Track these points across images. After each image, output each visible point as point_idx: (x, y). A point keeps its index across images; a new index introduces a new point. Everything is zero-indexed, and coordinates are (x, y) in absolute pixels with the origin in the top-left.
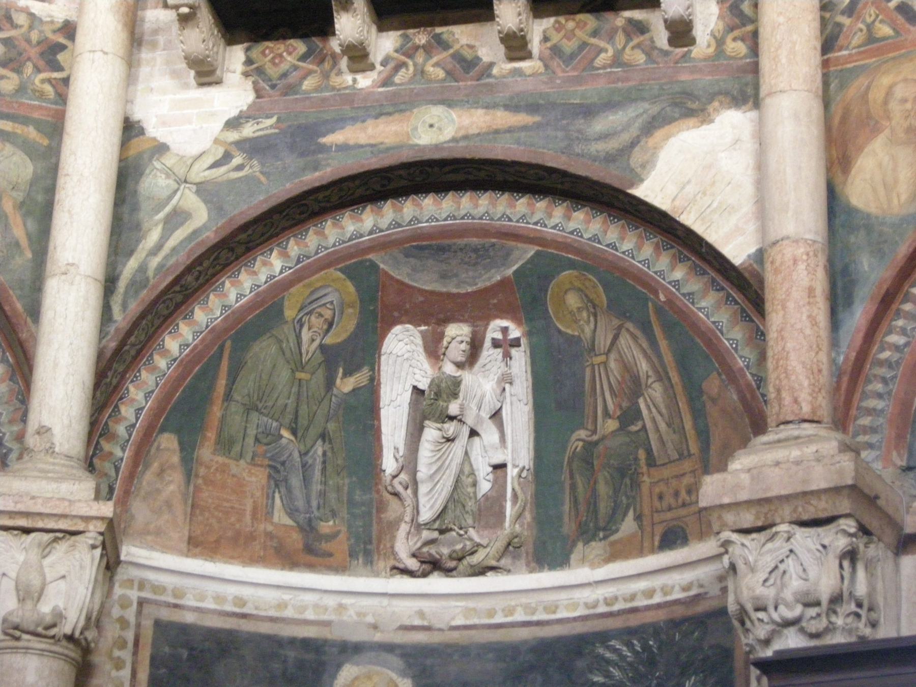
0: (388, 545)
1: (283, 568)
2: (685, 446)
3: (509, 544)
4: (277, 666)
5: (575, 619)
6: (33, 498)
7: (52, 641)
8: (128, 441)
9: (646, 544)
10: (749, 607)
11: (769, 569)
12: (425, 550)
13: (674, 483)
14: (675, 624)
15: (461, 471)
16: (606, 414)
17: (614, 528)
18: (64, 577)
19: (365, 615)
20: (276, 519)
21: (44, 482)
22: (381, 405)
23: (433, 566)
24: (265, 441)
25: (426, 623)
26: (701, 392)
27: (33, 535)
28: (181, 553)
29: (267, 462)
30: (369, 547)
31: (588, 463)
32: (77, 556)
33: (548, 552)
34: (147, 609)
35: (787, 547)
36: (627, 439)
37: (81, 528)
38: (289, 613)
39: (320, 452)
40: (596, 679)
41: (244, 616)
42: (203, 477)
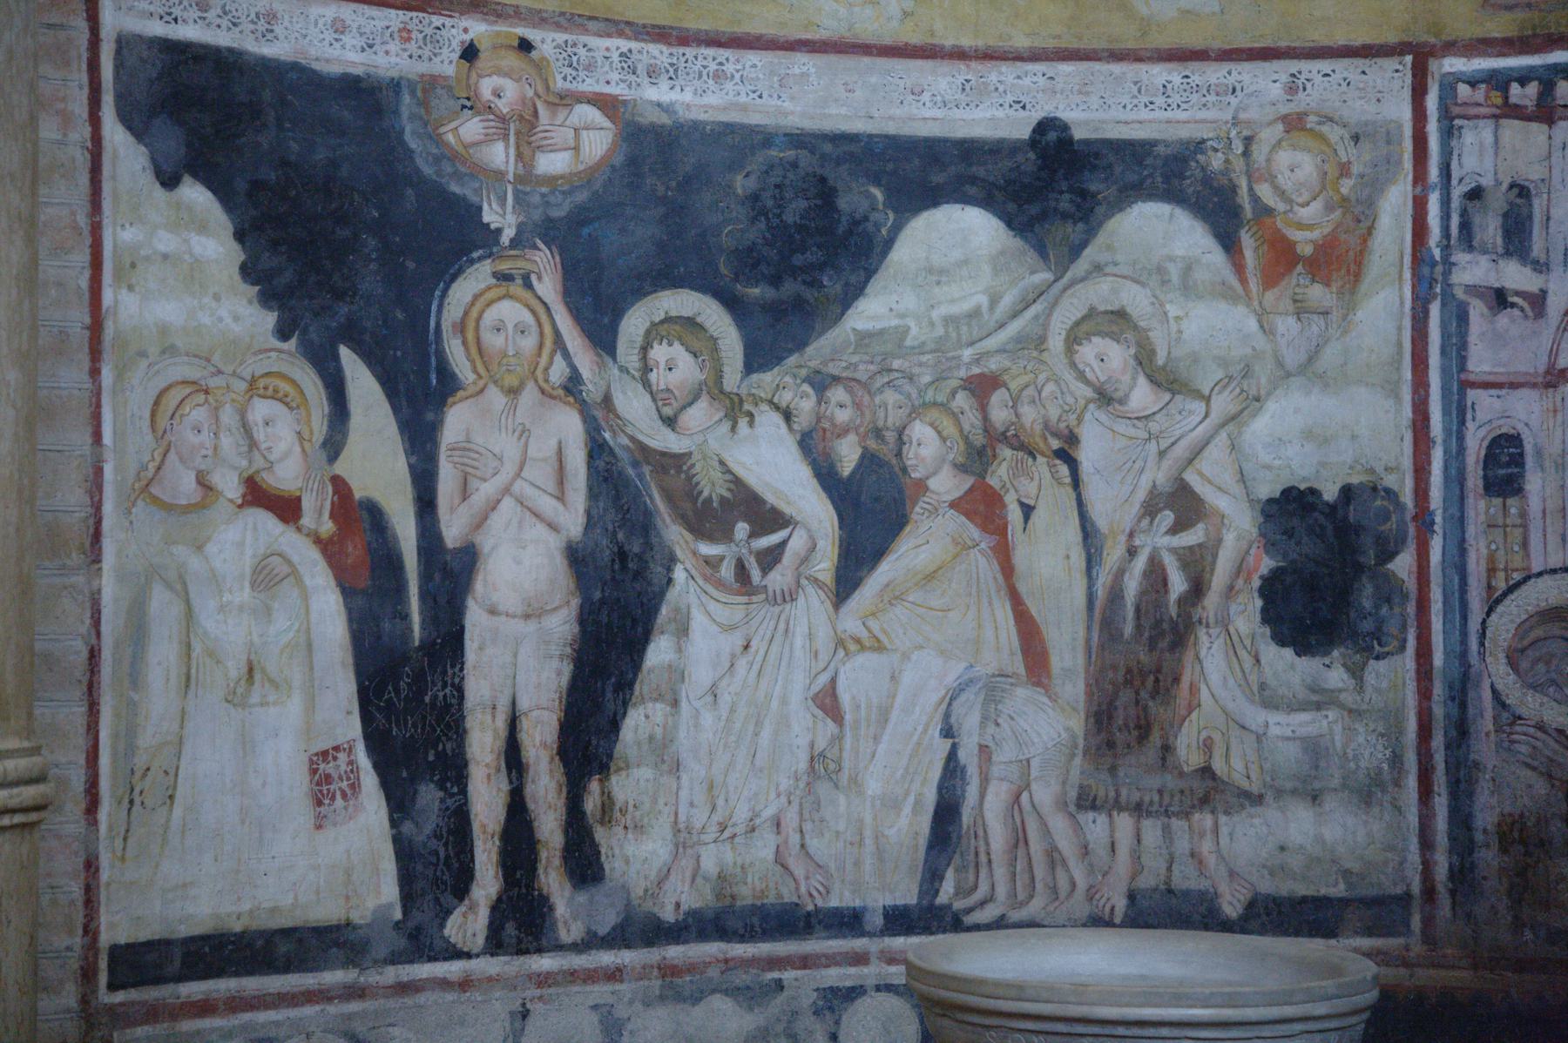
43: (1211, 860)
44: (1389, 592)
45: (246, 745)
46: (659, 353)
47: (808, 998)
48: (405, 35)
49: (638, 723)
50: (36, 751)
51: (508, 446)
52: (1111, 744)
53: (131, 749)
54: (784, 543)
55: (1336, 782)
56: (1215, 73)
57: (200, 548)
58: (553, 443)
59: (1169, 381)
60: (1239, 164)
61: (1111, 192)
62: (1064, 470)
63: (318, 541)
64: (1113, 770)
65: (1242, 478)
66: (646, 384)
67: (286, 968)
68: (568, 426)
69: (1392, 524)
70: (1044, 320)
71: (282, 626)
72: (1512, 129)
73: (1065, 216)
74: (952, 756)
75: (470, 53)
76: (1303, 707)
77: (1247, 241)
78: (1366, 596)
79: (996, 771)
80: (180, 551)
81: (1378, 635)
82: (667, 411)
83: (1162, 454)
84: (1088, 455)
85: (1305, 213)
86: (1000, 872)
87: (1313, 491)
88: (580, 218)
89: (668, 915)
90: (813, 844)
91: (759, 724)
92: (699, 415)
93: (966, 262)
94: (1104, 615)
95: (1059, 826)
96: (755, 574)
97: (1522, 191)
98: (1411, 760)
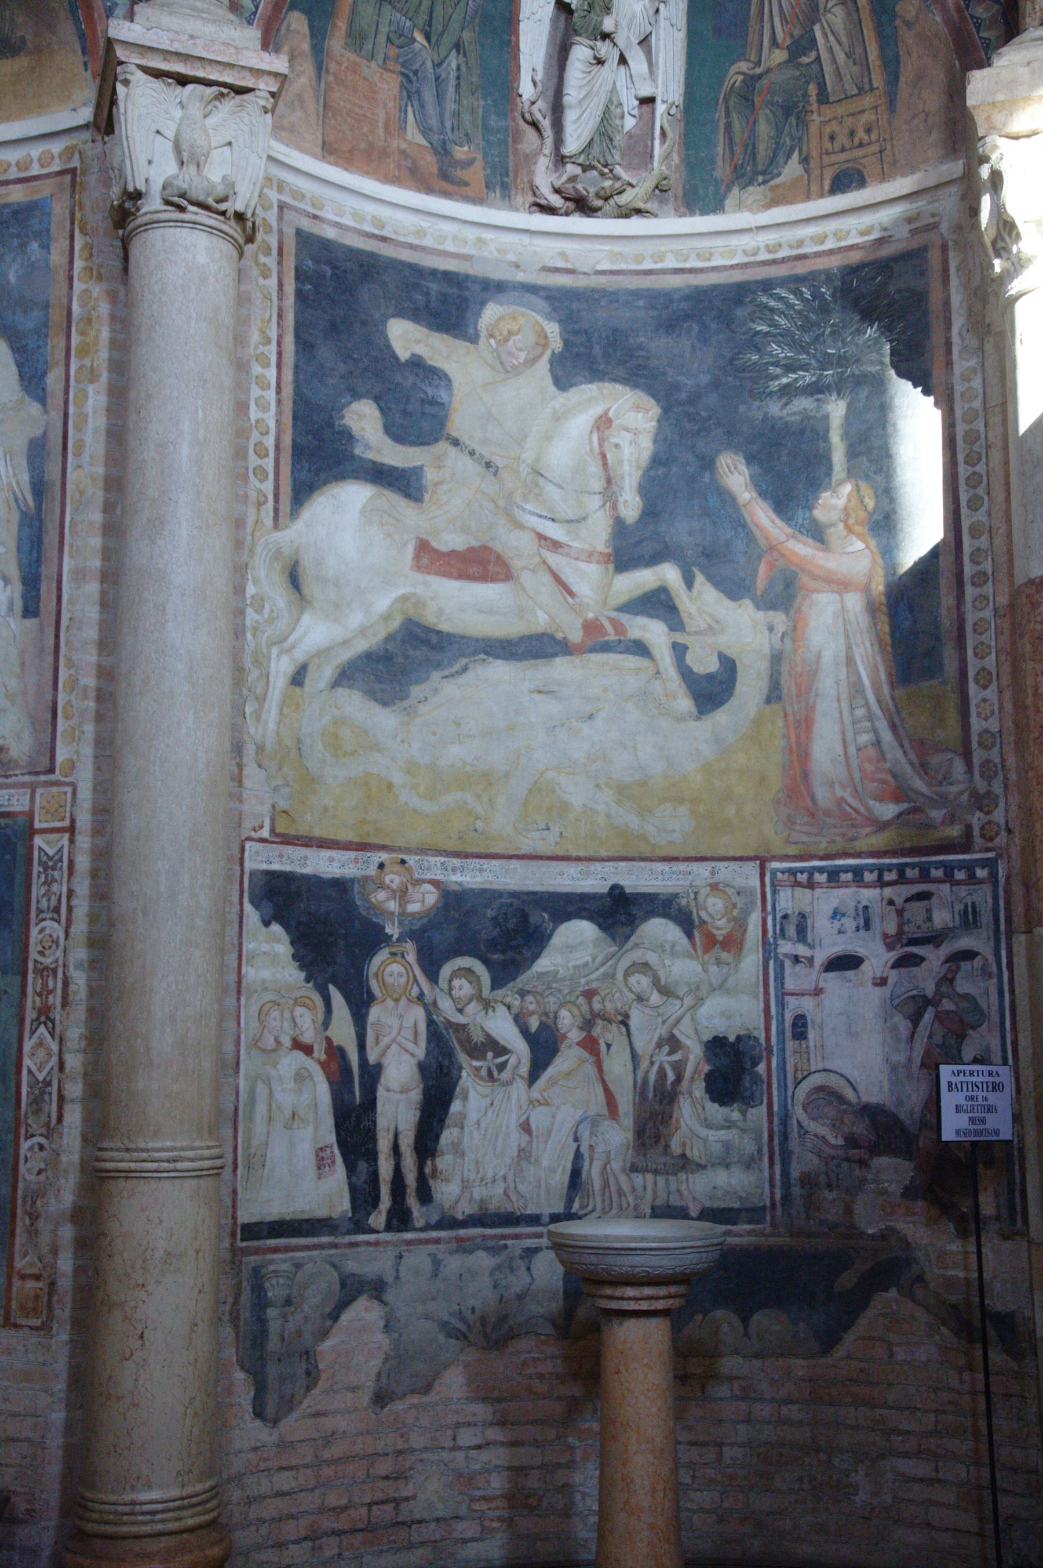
1: (419, 191)
2: (866, 80)
5: (732, 267)
6: (192, 37)
8: (255, 14)
9: (813, 188)
12: (569, 186)
13: (850, 120)
15: (611, 101)
16: (774, 43)
18: (230, 144)
19: (506, 252)
20: (409, 137)
21: (199, 23)
22: (521, 18)
24: (397, 42)
25: (569, 266)
26: (894, 15)
27: (190, 87)
28: (315, 156)
29: (398, 68)
31: (747, 100)
32: (246, 119)
33: (699, 194)
34: (288, 215)
36: (797, 73)
37: (250, 85)
38: (428, 242)
39: (454, 66)
41: (384, 239)
42: (335, 74)
43: (686, 1193)
44: (756, 1079)
45: (292, 1145)
46: (456, 983)
47: (518, 1252)
48: (356, 861)
49: (447, 1136)
50: (220, 1146)
51: (394, 1022)
52: (644, 1145)
53: (249, 1147)
54: (507, 1061)
55: (736, 1159)
56: (682, 866)
57: (275, 1067)
59: (666, 992)
60: (693, 903)
61: (641, 914)
62: (624, 1029)
64: (645, 1155)
65: (696, 1032)
66: (451, 995)
67: (306, 1236)
68: (419, 1014)
70: (615, 967)
71: (306, 1097)
72: (799, 891)
73: (622, 924)
74: (578, 1150)
75: (381, 866)
76: (723, 1128)
77: (697, 934)
79: (596, 1156)
81: (752, 1097)
83: (664, 1022)
84: (635, 1021)
85: (719, 923)
86: (598, 1199)
87: (725, 1038)
88: (424, 929)
89: (460, 1217)
90: (520, 1187)
92: (472, 1008)
93: (582, 943)
94: (641, 1089)
95: (622, 1178)
97: (803, 916)
98: (765, 1149)
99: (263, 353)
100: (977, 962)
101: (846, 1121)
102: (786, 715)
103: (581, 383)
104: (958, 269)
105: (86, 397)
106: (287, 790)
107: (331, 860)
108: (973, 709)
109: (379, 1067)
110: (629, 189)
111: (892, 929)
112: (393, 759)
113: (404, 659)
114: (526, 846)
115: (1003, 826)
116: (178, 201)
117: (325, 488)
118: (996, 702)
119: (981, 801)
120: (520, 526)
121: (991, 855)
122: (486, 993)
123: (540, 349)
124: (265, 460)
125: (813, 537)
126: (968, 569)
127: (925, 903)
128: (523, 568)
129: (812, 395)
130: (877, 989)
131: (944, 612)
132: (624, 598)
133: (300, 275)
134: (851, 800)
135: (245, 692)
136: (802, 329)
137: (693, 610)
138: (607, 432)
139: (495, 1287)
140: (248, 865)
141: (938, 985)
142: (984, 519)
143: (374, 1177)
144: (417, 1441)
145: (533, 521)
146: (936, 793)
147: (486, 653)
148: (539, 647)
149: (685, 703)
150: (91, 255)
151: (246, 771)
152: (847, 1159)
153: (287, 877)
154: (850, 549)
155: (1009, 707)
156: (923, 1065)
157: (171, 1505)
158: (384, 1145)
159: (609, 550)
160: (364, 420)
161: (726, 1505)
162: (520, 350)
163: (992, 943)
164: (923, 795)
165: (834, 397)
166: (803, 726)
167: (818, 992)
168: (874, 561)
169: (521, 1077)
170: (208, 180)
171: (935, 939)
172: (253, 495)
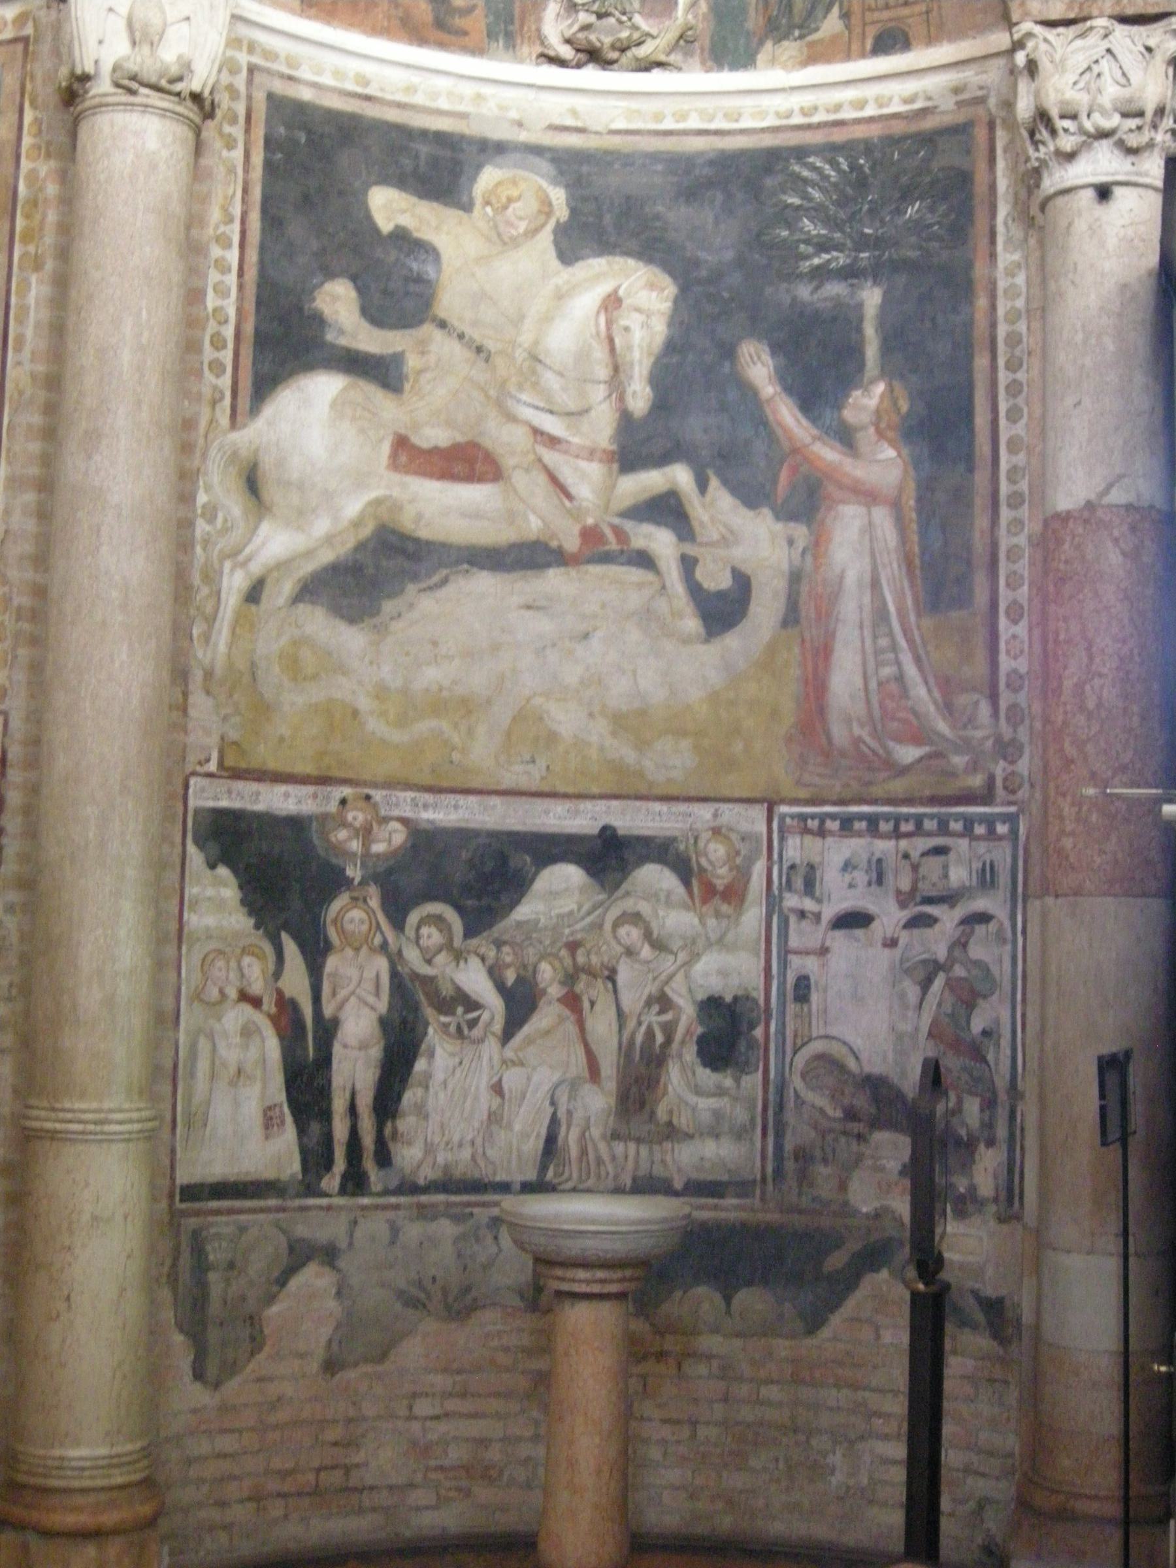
0: (533, 27)
1: (411, 42)
3: (681, 37)
4: (407, 161)
7: (176, 99)
10: (1054, 113)
11: (1081, 70)
12: (581, 35)
14: (891, 141)
17: (813, 26)
18: (188, 19)
23: (593, 56)
25: (580, 124)
28: (292, 11)
30: (511, 28)
33: (728, 46)
34: (258, 78)
35: (1105, 44)
38: (419, 99)
40: (790, 201)
41: (368, 98)
44: (752, 1044)
45: (237, 1104)
46: (425, 931)
47: (485, 1220)
48: (315, 796)
49: (409, 1097)
51: (353, 973)
56: (682, 807)
58: (373, 974)
59: (659, 945)
60: (691, 848)
62: (610, 985)
63: (269, 1016)
64: (628, 1122)
65: (690, 990)
68: (382, 964)
69: (755, 1014)
71: (253, 1053)
72: (808, 839)
74: (554, 1114)
75: (343, 802)
76: (714, 1095)
78: (742, 1046)
79: (575, 1121)
80: (211, 1021)
81: (747, 1063)
82: (428, 957)
83: (655, 979)
84: (622, 977)
85: (723, 871)
88: (390, 872)
89: (421, 1182)
90: (489, 1152)
91: (465, 1097)
93: (567, 889)
94: (626, 1051)
95: (602, 1147)
96: (466, 1031)
97: (811, 867)
98: (759, 1121)
99: (224, 233)
100: (992, 926)
101: (847, 1092)
102: (803, 641)
103: (588, 257)
104: (1005, 151)
105: (25, 285)
106: (236, 719)
107: (287, 795)
108: (1002, 646)
109: (335, 1023)
110: (649, 40)
111: (905, 884)
112: (360, 683)
113: (376, 571)
114: (508, 780)
115: (1026, 779)
116: (130, 83)
117: (290, 381)
118: (1026, 639)
119: (1007, 749)
120: (511, 418)
121: (1013, 809)
122: (458, 941)
123: (542, 218)
124: (223, 353)
125: (841, 440)
126: (1004, 488)
127: (942, 858)
128: (515, 467)
129: (846, 279)
130: (887, 951)
131: (977, 535)
132: (627, 503)
133: (270, 143)
134: (868, 739)
135: (192, 612)
136: (839, 204)
137: (705, 518)
138: (615, 313)
139: (459, 1256)
140: (192, 803)
141: (951, 949)
142: (1023, 433)
143: (328, 1139)
144: (369, 1409)
145: (527, 413)
146: (960, 737)
147: (472, 563)
148: (528, 557)
149: (692, 624)
150: (40, 131)
151: (191, 699)
152: (845, 1133)
153: (236, 816)
154: (881, 456)
155: (1037, 648)
156: (930, 1035)
157: (101, 1463)
158: (339, 1105)
159: (614, 447)
160: (338, 303)
161: (697, 1482)
162: (521, 219)
163: (1008, 906)
164: (947, 740)
165: (869, 283)
166: (821, 655)
167: (823, 951)
168: (905, 471)
169: (493, 1034)
170: (162, 62)
171: (949, 899)
172: (207, 391)
